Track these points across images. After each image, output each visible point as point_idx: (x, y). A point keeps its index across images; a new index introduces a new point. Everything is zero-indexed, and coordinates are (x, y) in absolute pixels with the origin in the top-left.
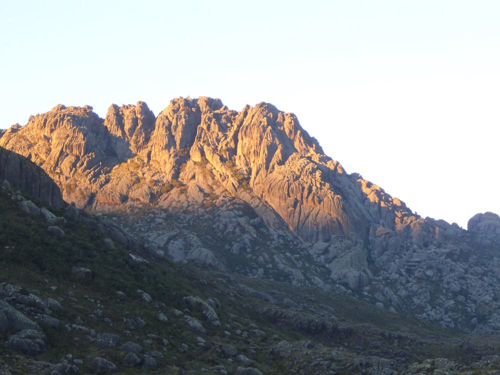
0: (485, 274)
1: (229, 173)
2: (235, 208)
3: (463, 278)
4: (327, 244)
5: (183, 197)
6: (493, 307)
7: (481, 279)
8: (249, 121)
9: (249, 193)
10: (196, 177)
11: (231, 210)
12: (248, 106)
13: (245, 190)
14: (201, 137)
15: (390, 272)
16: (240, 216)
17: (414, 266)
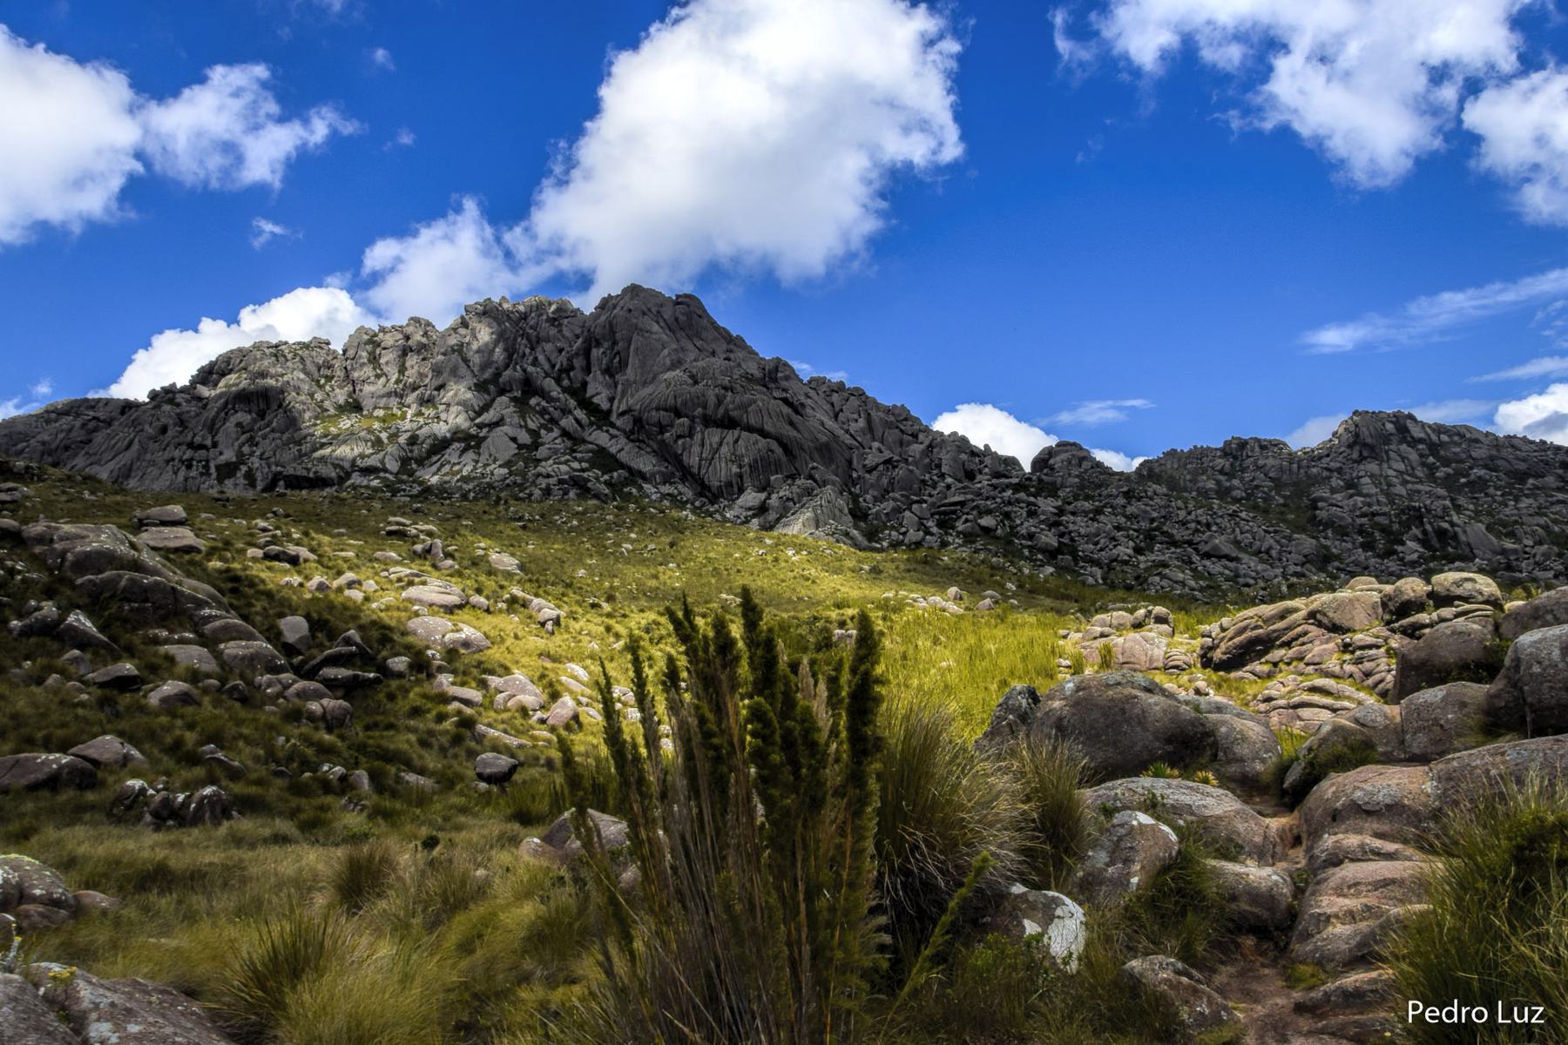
0: (1099, 511)
1: (572, 403)
2: (575, 458)
3: (1057, 524)
4: (763, 496)
5: (470, 455)
6: (1142, 566)
7: (1093, 519)
9: (607, 431)
10: (508, 420)
11: (566, 462)
13: (600, 428)
15: (903, 530)
16: (583, 470)
17: (954, 512)
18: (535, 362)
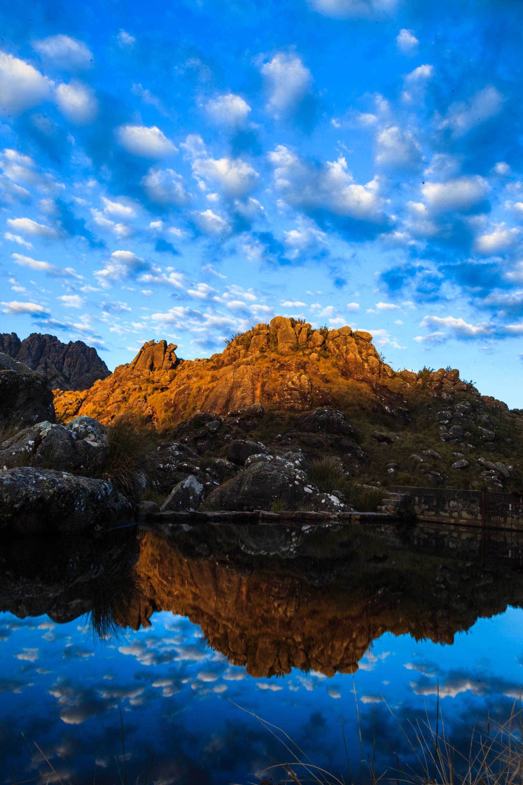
8: (72, 350)
12: (71, 342)
13: (67, 383)
14: (45, 355)
18: (49, 358)
